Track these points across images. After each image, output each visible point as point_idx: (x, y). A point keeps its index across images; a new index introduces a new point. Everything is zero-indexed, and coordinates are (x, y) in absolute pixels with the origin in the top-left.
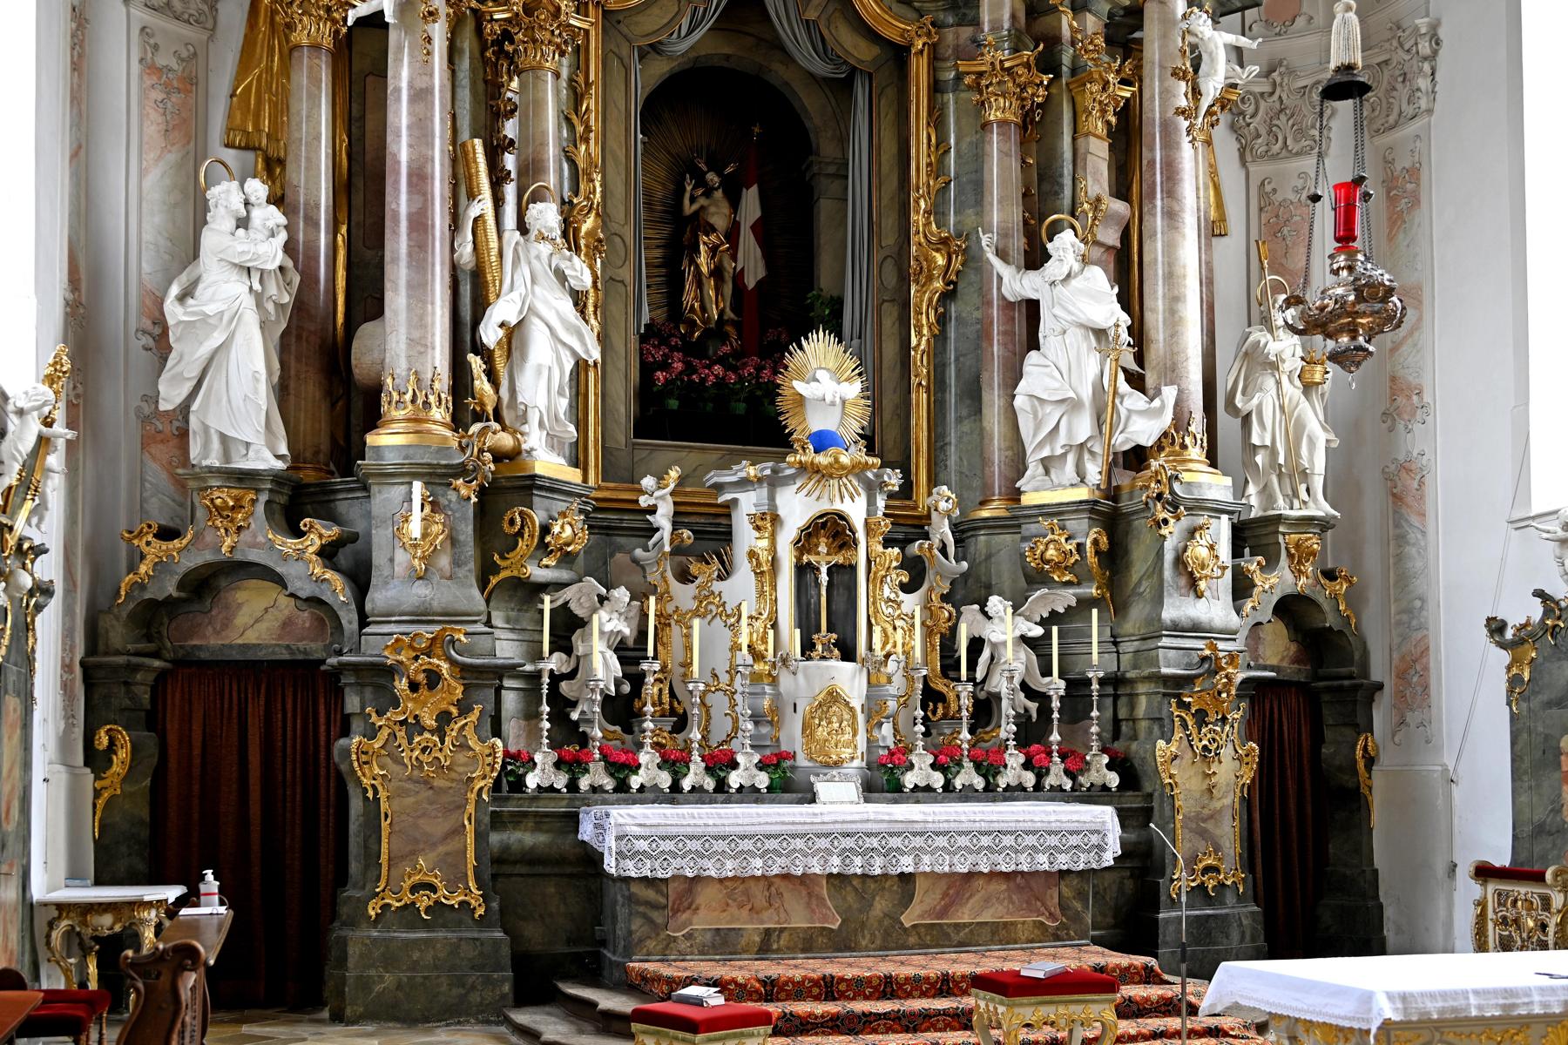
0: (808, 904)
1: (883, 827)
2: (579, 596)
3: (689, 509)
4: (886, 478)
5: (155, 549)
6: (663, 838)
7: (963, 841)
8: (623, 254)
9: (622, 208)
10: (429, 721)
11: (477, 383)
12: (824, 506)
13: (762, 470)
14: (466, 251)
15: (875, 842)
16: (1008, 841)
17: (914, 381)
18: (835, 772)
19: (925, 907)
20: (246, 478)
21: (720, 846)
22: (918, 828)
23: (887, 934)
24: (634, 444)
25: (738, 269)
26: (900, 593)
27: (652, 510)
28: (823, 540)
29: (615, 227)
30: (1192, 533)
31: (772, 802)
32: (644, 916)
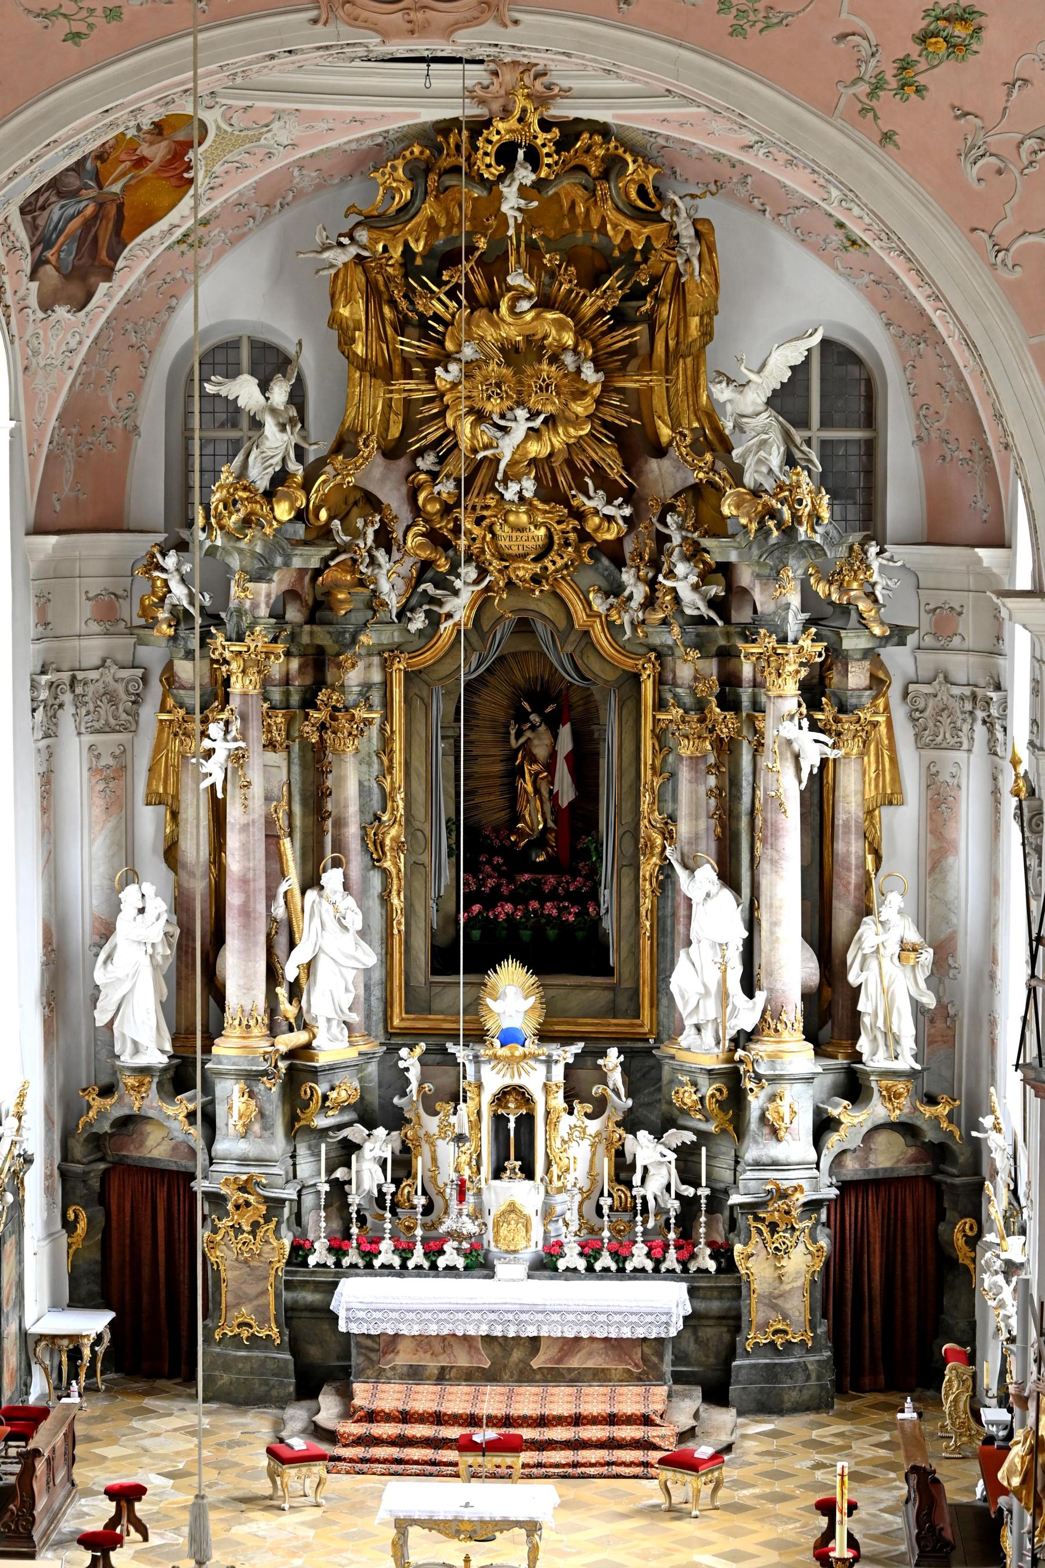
0: (469, 1352)
1: (516, 1307)
2: (356, 1133)
5: (97, 1103)
6: (375, 1310)
7: (570, 1317)
9: (423, 810)
10: (247, 1228)
11: (282, 1007)
12: (507, 1081)
14: (279, 911)
15: (510, 1317)
16: (602, 1318)
19: (547, 1357)
20: (144, 1071)
21: (411, 1316)
22: (540, 1308)
23: (521, 1372)
27: (407, 1069)
30: (772, 1098)
31: (467, 1277)
32: (365, 1355)
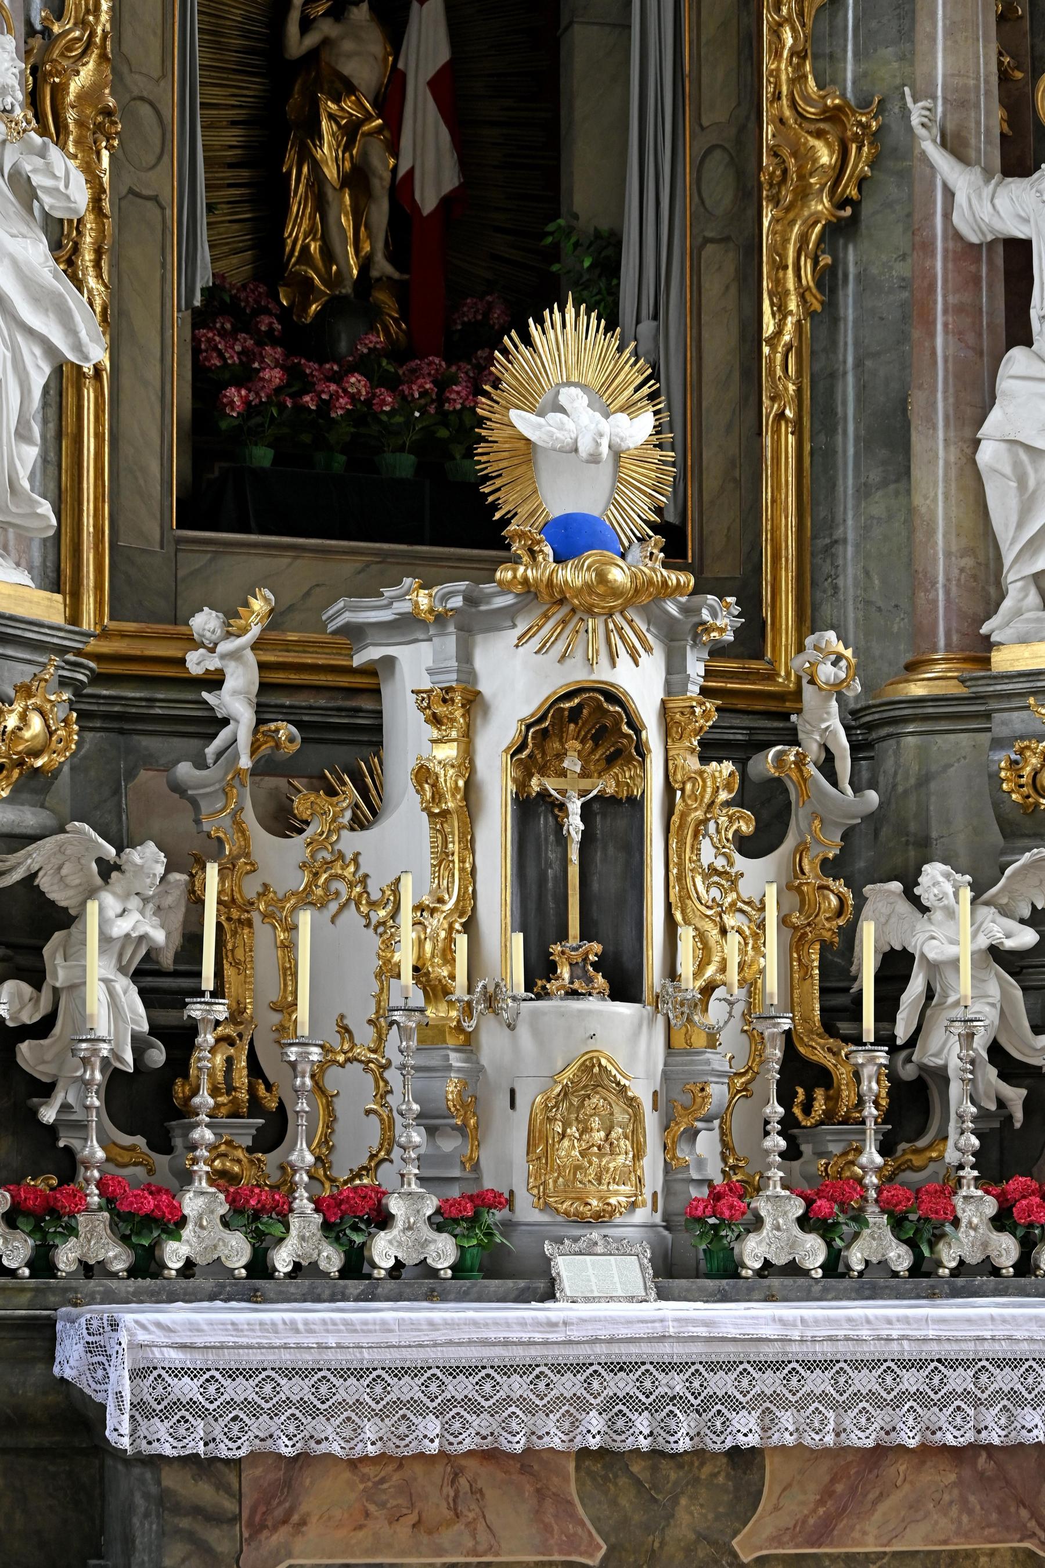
0: (538, 1513)
1: (695, 1351)
3: (294, 678)
4: (706, 615)
6: (232, 1374)
7: (864, 1381)
8: (157, 141)
9: (155, 44)
12: (576, 674)
13: (446, 597)
15: (677, 1384)
16: (959, 1380)
17: (769, 409)
18: (595, 1235)
19: (785, 1520)
21: (351, 1390)
22: (770, 1352)
24: (179, 541)
25: (402, 172)
26: (737, 857)
27: (215, 681)
28: (572, 745)
29: (138, 84)
31: (463, 1297)
32: (191, 1537)
